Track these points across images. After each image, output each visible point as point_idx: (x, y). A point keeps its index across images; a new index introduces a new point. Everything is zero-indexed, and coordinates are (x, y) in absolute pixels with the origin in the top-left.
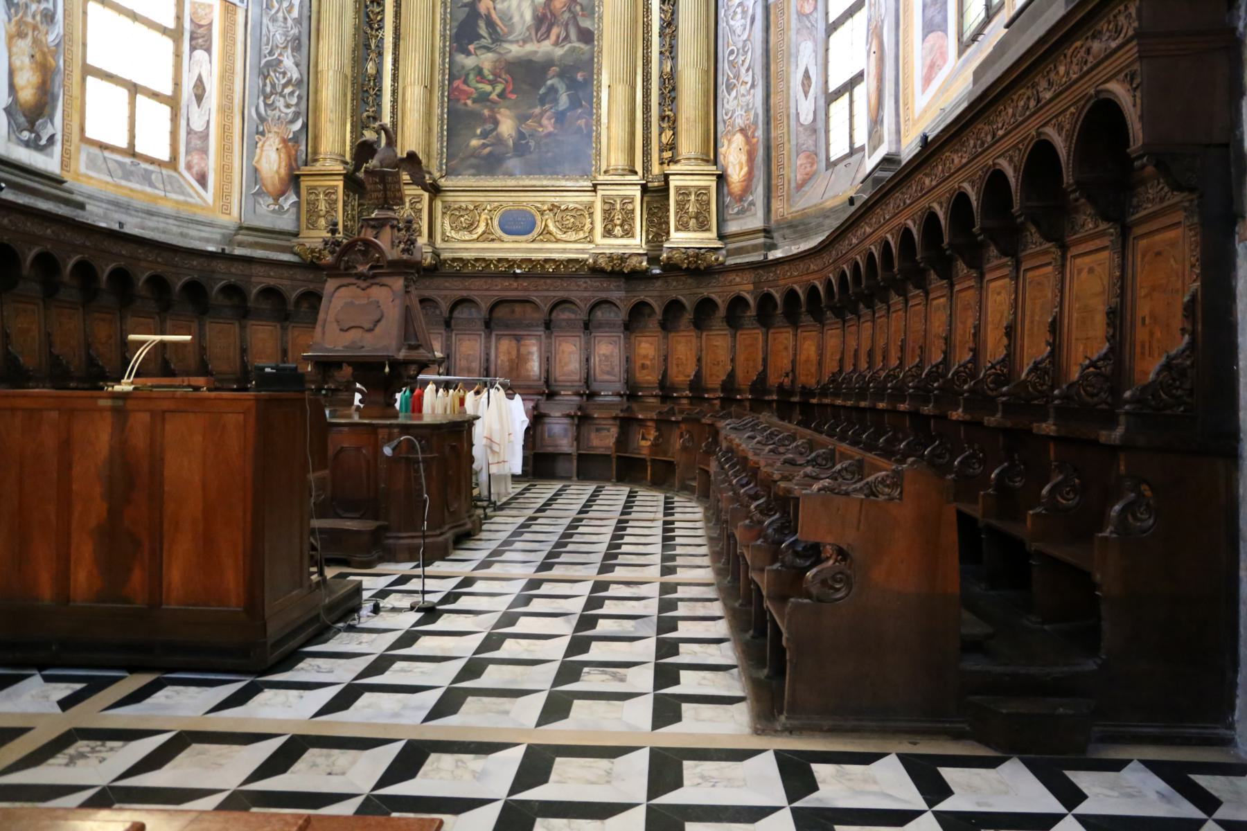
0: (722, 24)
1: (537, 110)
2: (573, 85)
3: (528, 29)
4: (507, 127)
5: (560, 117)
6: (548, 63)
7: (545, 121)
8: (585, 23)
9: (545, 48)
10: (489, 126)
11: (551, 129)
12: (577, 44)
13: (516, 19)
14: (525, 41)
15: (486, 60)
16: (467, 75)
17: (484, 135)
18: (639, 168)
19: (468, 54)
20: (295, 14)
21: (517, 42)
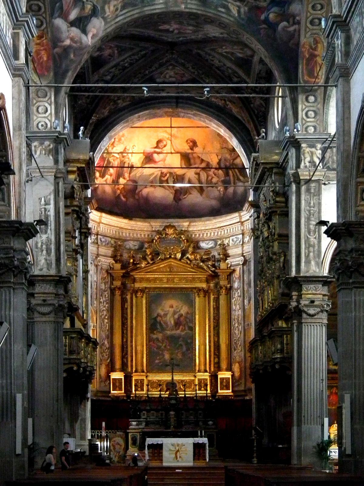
0: (232, 331)
1: (177, 351)
2: (187, 344)
3: (173, 327)
4: (167, 356)
5: (183, 354)
6: (179, 337)
7: (179, 355)
8: (191, 325)
9: (178, 332)
10: (161, 357)
11: (180, 357)
12: (188, 331)
13: (169, 323)
14: (172, 330)
15: (160, 336)
16: (154, 341)
17: (160, 359)
18: (208, 369)
19: (154, 334)
20: (107, 328)
21: (169, 330)
